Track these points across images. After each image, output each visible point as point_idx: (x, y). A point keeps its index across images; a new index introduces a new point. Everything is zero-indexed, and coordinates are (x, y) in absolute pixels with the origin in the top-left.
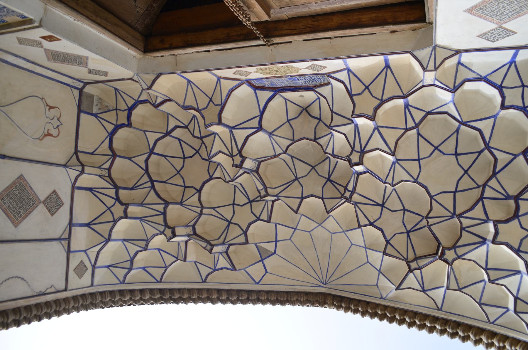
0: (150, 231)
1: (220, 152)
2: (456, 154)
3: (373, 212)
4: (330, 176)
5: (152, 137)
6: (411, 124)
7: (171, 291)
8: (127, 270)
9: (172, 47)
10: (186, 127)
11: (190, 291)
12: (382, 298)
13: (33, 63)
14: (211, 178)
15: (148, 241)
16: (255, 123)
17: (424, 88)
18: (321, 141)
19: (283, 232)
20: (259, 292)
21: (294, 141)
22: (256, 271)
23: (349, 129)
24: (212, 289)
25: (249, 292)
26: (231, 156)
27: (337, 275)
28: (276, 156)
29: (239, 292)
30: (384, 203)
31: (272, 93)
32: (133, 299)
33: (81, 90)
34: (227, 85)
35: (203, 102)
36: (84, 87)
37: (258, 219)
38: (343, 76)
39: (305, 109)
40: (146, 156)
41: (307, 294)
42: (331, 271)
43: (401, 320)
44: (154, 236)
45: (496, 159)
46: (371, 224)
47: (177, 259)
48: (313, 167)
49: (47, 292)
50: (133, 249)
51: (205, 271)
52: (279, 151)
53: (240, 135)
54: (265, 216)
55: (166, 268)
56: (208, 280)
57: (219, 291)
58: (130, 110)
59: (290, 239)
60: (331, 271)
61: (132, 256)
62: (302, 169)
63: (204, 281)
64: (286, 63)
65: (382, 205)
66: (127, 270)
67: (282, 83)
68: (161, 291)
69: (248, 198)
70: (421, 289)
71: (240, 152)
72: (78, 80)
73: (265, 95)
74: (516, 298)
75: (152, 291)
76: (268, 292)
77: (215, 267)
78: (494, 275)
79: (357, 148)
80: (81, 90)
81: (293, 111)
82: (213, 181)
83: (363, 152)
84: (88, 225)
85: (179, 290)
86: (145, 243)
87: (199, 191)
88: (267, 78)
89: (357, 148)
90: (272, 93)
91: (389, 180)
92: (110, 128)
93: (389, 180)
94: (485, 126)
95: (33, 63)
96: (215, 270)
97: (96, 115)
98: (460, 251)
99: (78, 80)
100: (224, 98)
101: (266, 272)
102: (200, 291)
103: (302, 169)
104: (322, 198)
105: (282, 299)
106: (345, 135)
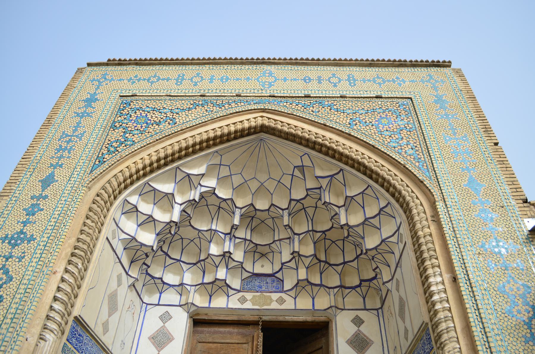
0: (359, 230)
1: (307, 257)
2: (182, 239)
3: (223, 205)
4: (252, 219)
5: (354, 264)
6: (202, 263)
7: (365, 174)
8: (384, 210)
9: (312, 322)
10: (331, 265)
11: (353, 167)
12: (217, 152)
13: (383, 345)
14: (324, 232)
15: (363, 223)
16: (284, 267)
17: (195, 284)
18: (253, 245)
19: (286, 181)
20: (307, 146)
21: (269, 245)
22: (307, 162)
23: (232, 264)
24: (339, 161)
25: (313, 148)
26: (300, 255)
27: (253, 148)
28: (280, 240)
29: (320, 151)
30: (219, 208)
31: (276, 275)
32: (388, 185)
33: (381, 308)
34: (292, 293)
35: (309, 288)
36: (379, 308)
37: (298, 201)
38: (231, 292)
39: (263, 255)
40: (361, 256)
41: (274, 134)
42: (258, 149)
43: (202, 143)
44: (358, 226)
45: (162, 250)
46: (225, 200)
47: (352, 197)
48: (263, 222)
49: (398, 269)
50: (375, 222)
51: (340, 177)
52: (278, 243)
53: (292, 264)
54: (293, 203)
55: (362, 193)
56: (339, 169)
57: (333, 157)
58: (359, 286)
59: (284, 174)
60: (258, 149)
61: (378, 216)
62: (270, 222)
63: (341, 170)
64: (254, 309)
65: (219, 207)
66: (384, 210)
67: (267, 283)
68: (371, 177)
69: (305, 210)
70: (190, 176)
71: (294, 257)
72: (378, 316)
73: (279, 275)
74: (137, 211)
75: (377, 181)
76: (300, 144)
77: (332, 178)
78: (151, 219)
79: (227, 258)
80: (381, 308)
81: (270, 256)
82: (325, 229)
83: (224, 255)
84: (393, 253)
85: (359, 170)
86: (366, 223)
87: (332, 227)
88: (271, 292)
89: (227, 258)
90: (276, 275)
91: (213, 232)
92: (375, 281)
93: (213, 232)
94: (170, 261)
95: (383, 345)
96: (332, 176)
97: (381, 290)
98: (168, 226)
99: (378, 316)
100: (295, 289)
101: (301, 157)
102: (346, 164)
103: (270, 222)
104: (256, 210)
105: (291, 137)
106: (234, 261)
